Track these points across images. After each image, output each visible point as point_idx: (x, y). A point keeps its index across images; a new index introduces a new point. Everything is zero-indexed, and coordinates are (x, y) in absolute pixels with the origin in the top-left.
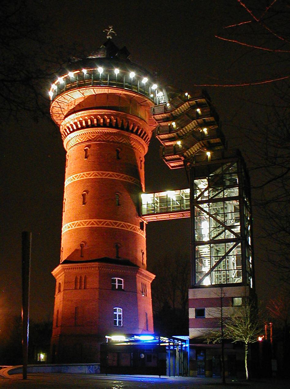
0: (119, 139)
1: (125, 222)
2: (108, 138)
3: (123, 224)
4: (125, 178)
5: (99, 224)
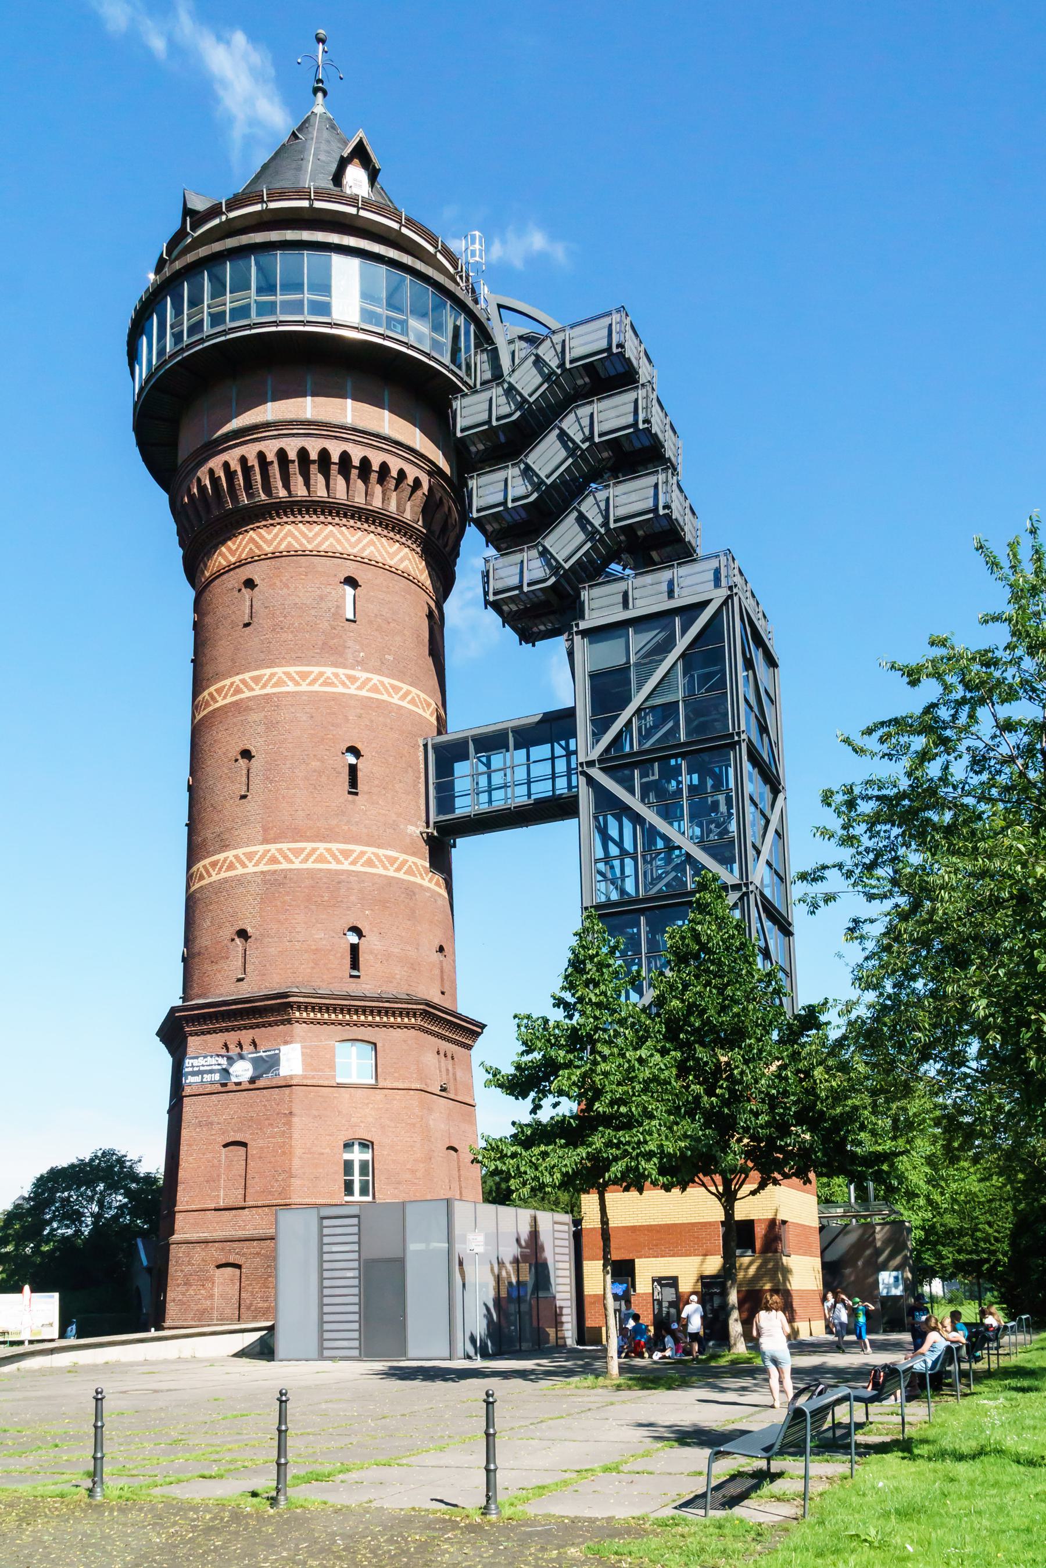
0: (353, 539)
1: (379, 847)
4: (375, 689)
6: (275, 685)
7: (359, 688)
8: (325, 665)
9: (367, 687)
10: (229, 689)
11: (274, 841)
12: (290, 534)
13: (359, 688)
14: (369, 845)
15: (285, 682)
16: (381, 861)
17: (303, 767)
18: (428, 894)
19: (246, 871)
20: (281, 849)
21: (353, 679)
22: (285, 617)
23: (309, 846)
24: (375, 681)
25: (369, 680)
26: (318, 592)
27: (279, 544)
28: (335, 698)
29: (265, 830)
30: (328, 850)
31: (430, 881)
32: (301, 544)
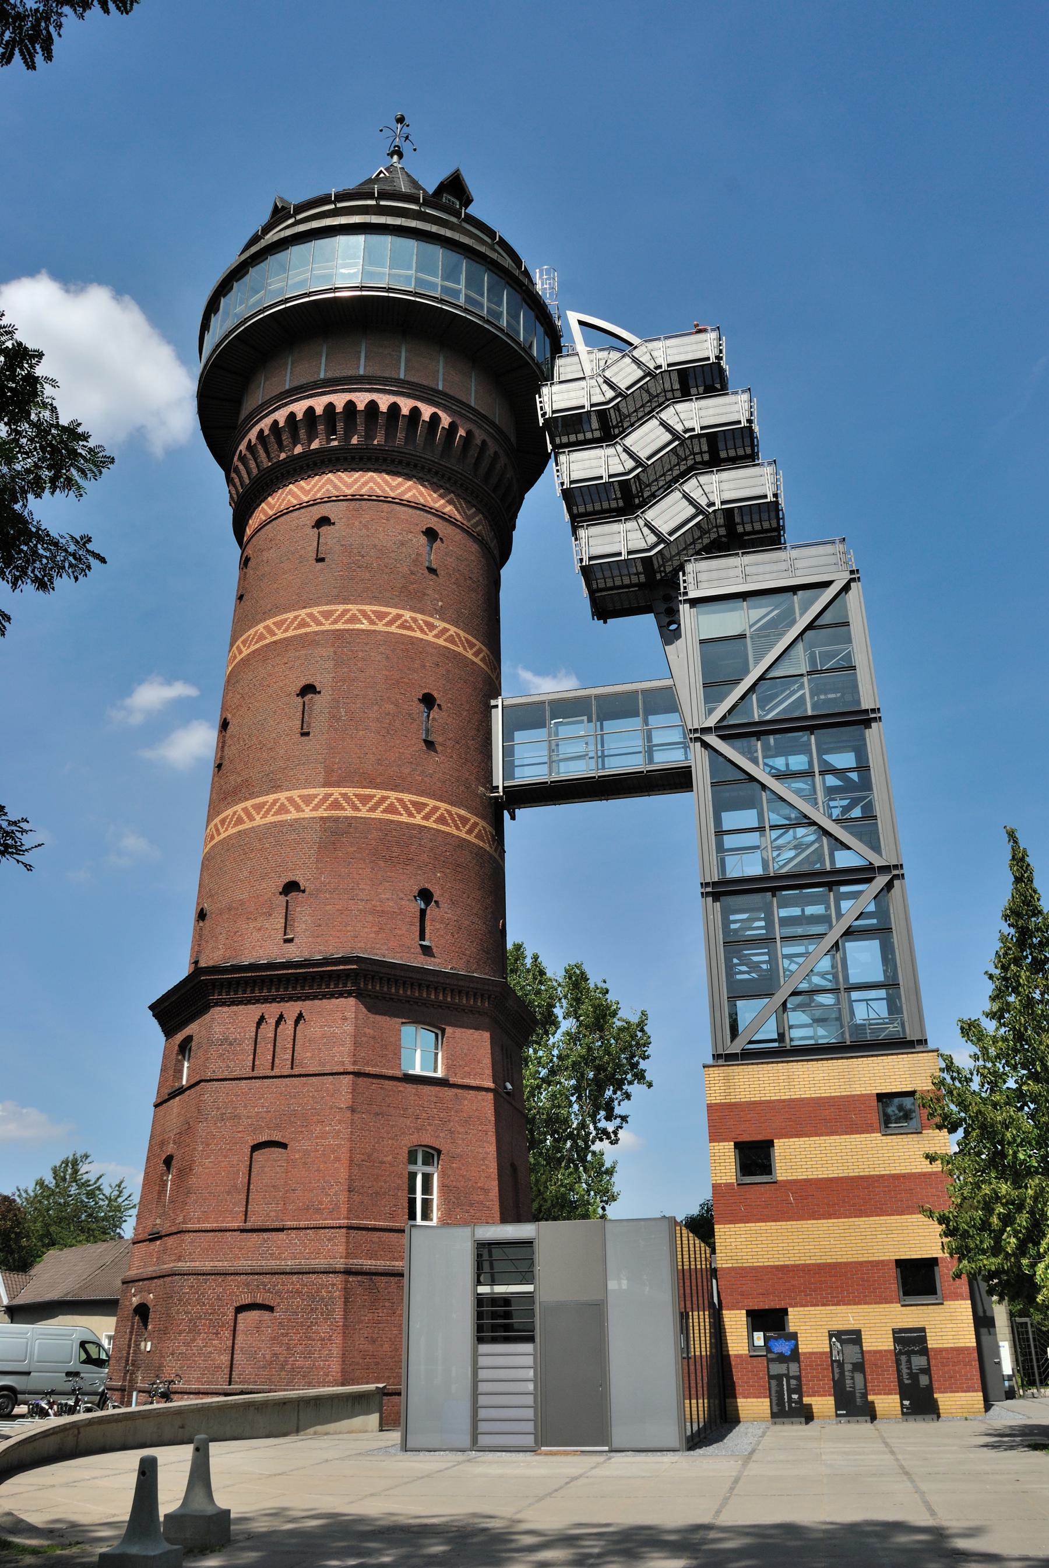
1: (452, 804)
3: (446, 810)
4: (451, 640)
6: (350, 621)
8: (403, 608)
9: (445, 637)
10: (292, 622)
11: (338, 785)
12: (372, 479)
13: (436, 636)
14: (441, 801)
15: (359, 620)
16: (453, 820)
17: (376, 708)
19: (301, 815)
20: (346, 794)
21: (431, 627)
22: (363, 556)
23: (379, 793)
24: (451, 632)
25: (446, 630)
27: (360, 488)
28: (412, 641)
29: (329, 771)
30: (400, 800)
31: (496, 850)
32: (383, 490)
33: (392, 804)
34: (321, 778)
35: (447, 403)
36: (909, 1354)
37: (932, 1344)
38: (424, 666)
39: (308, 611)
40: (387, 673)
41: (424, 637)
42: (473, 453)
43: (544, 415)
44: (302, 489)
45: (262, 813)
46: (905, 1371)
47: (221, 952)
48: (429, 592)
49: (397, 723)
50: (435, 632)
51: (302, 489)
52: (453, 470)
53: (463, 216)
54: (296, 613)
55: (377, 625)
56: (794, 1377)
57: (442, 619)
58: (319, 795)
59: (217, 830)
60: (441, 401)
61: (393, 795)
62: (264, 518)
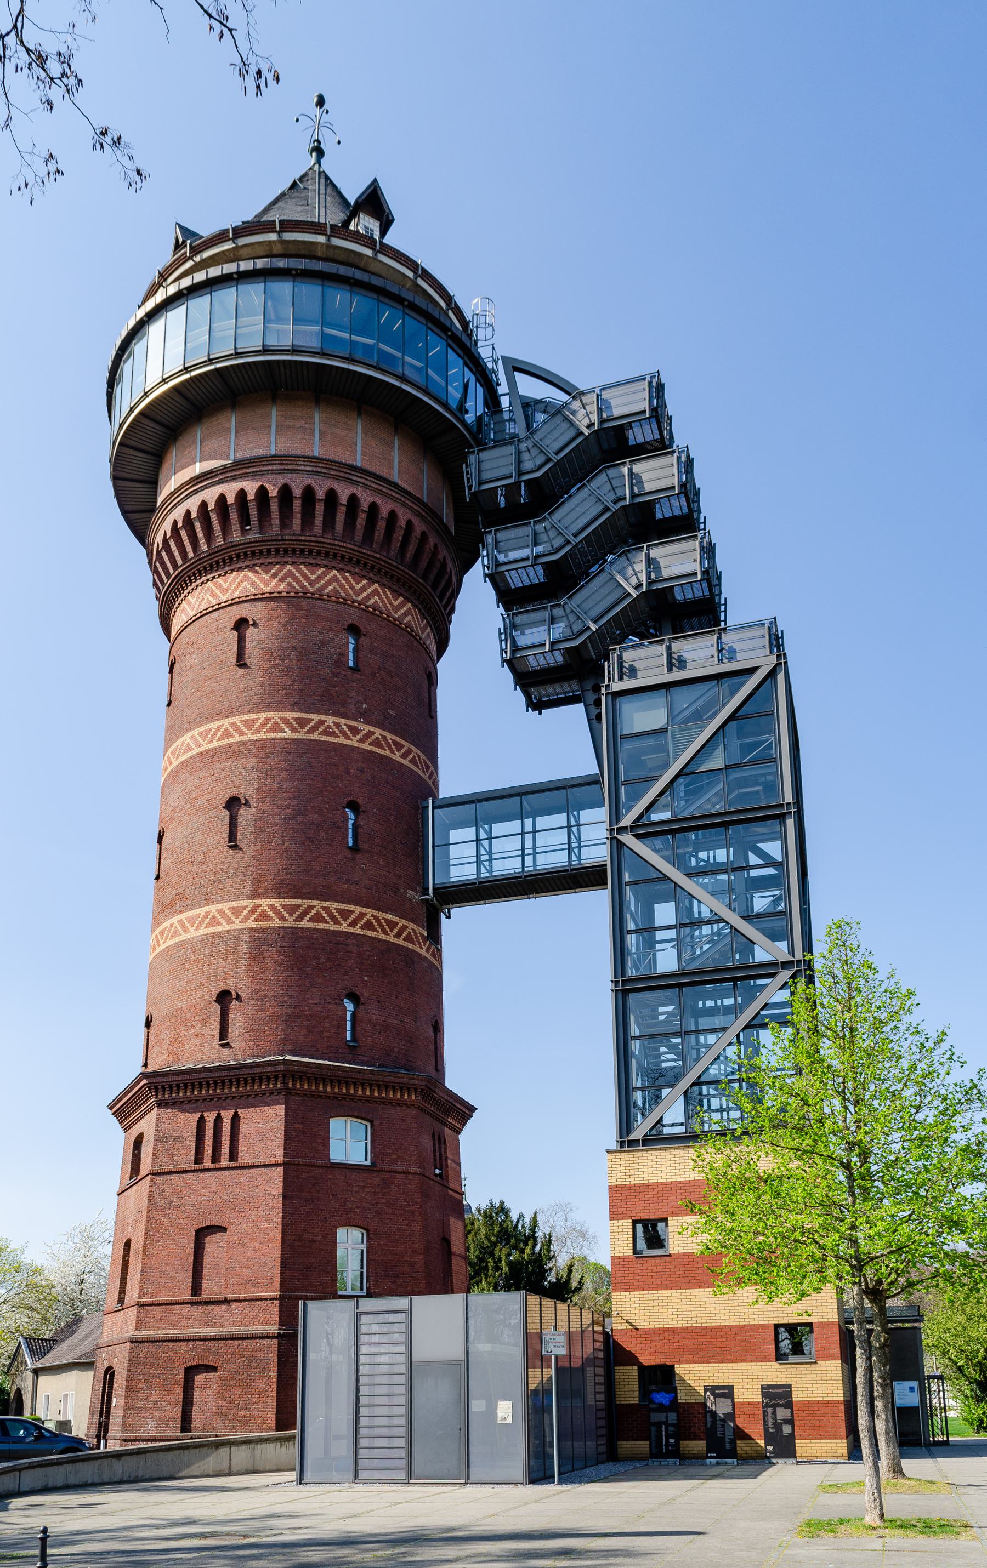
2: (320, 578)
4: (376, 743)
5: (287, 915)
7: (361, 741)
9: (370, 740)
13: (361, 741)
18: (425, 964)
21: (355, 731)
25: (370, 733)
26: (320, 637)
33: (318, 913)
34: (249, 890)
35: (366, 482)
36: (775, 1407)
37: (795, 1398)
38: (349, 773)
39: (231, 720)
40: (310, 782)
41: (348, 742)
42: (399, 535)
43: (470, 488)
44: (219, 586)
45: (196, 925)
46: (770, 1421)
47: (165, 1057)
48: (353, 694)
49: (322, 832)
50: (358, 737)
51: (219, 586)
52: (376, 558)
53: (378, 248)
54: (220, 723)
55: (300, 732)
56: (672, 1425)
57: (367, 722)
58: (247, 906)
59: (158, 942)
60: (359, 480)
61: (319, 904)
62: (186, 620)
